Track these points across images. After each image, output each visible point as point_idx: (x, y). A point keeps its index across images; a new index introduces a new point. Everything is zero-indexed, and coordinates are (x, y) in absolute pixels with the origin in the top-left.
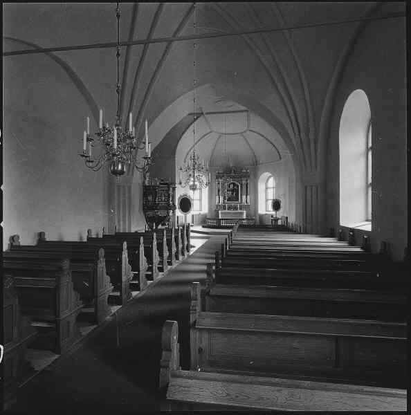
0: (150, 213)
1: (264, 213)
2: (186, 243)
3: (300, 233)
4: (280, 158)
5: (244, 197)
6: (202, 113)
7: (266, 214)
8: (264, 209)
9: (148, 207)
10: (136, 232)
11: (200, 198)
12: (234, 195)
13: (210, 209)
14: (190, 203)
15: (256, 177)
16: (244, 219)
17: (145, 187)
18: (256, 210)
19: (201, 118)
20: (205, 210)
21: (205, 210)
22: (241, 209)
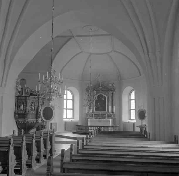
0: (21, 120)
1: (128, 121)
2: (49, 147)
3: (149, 140)
4: (140, 75)
5: (110, 108)
6: (73, 36)
7: (129, 122)
8: (128, 119)
9: (19, 114)
10: (6, 137)
11: (69, 107)
13: (81, 117)
14: (52, 111)
16: (110, 126)
19: (73, 39)
20: (77, 119)
21: (77, 119)
22: (108, 117)
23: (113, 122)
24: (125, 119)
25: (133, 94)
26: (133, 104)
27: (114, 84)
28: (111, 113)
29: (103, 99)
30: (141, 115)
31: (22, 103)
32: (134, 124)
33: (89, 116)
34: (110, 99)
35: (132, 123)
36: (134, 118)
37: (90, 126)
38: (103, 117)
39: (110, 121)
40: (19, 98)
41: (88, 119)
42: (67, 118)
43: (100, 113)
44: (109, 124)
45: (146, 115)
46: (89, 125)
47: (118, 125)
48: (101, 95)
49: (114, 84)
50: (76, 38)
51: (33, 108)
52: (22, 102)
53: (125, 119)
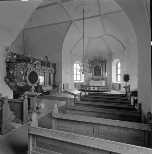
0: (11, 84)
5: (104, 73)
7: (116, 83)
12: (97, 71)
16: (104, 86)
17: (7, 63)
18: (111, 80)
20: (83, 81)
21: (83, 81)
22: (102, 80)
23: (106, 83)
24: (114, 81)
25: (119, 64)
26: (119, 71)
27: (106, 58)
28: (104, 77)
29: (99, 68)
30: (126, 78)
31: (12, 68)
32: (120, 84)
33: (91, 79)
34: (104, 68)
35: (118, 83)
36: (120, 81)
37: (91, 86)
38: (99, 79)
39: (103, 82)
40: (9, 64)
41: (89, 81)
42: (76, 80)
43: (97, 77)
44: (103, 84)
45: (130, 78)
46: (90, 85)
47: (108, 85)
48: (98, 65)
49: (106, 58)
50: (76, 22)
52: (12, 67)
53: (114, 81)
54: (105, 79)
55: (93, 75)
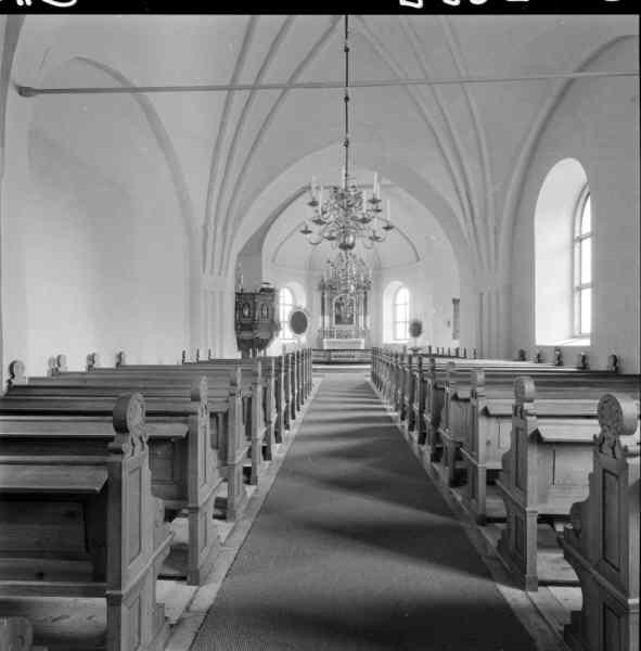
0: (246, 335)
4: (418, 260)
5: (361, 318)
7: (395, 344)
9: (242, 325)
15: (380, 290)
18: (379, 335)
46: (325, 348)
51: (265, 313)
54: (365, 333)
55: (331, 324)
